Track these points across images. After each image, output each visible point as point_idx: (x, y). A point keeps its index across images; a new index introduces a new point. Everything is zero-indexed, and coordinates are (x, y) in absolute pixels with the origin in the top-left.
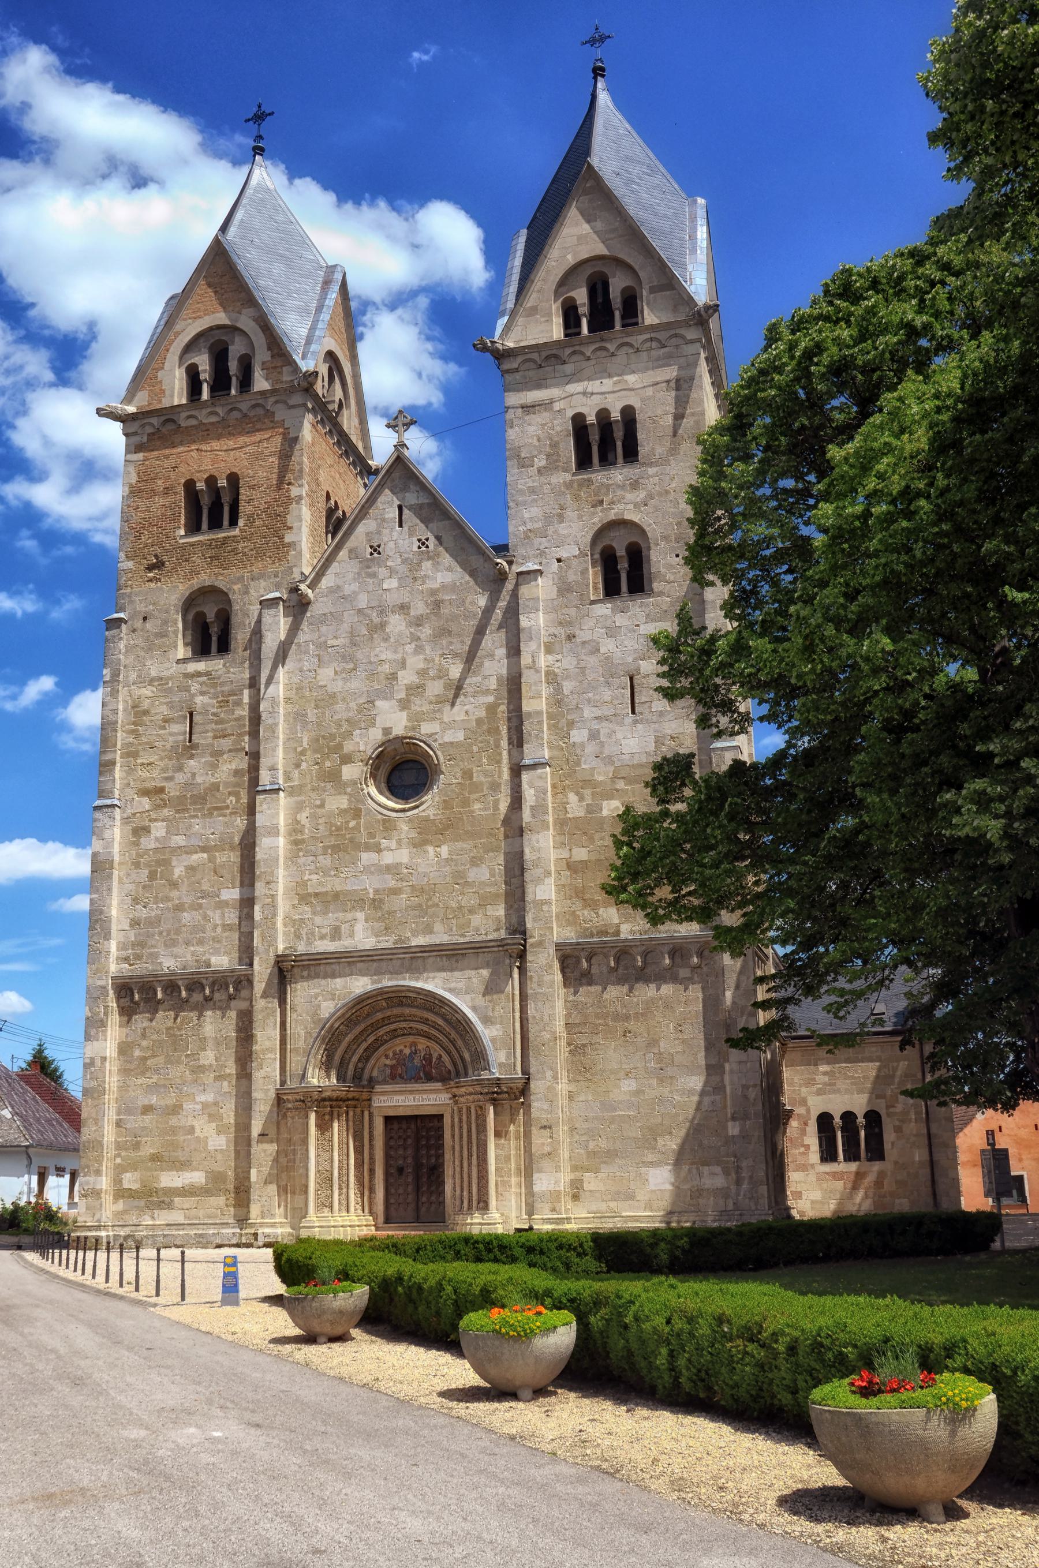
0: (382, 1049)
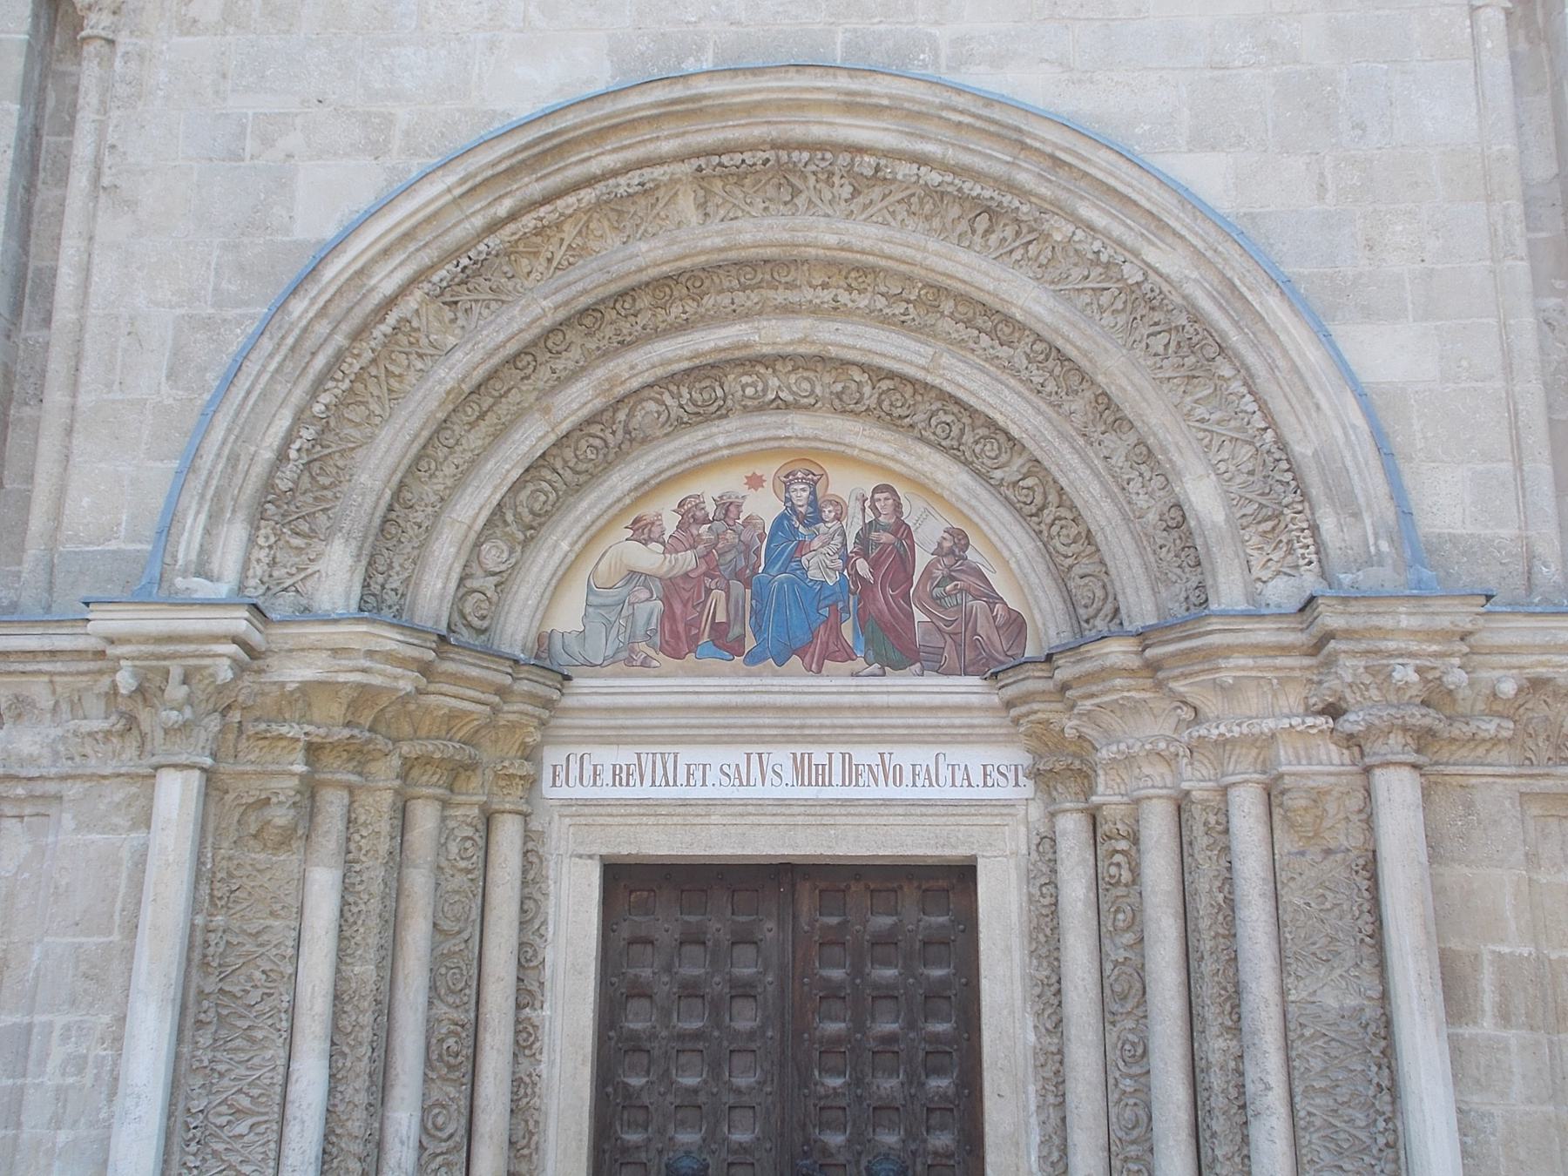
0: (621, 481)
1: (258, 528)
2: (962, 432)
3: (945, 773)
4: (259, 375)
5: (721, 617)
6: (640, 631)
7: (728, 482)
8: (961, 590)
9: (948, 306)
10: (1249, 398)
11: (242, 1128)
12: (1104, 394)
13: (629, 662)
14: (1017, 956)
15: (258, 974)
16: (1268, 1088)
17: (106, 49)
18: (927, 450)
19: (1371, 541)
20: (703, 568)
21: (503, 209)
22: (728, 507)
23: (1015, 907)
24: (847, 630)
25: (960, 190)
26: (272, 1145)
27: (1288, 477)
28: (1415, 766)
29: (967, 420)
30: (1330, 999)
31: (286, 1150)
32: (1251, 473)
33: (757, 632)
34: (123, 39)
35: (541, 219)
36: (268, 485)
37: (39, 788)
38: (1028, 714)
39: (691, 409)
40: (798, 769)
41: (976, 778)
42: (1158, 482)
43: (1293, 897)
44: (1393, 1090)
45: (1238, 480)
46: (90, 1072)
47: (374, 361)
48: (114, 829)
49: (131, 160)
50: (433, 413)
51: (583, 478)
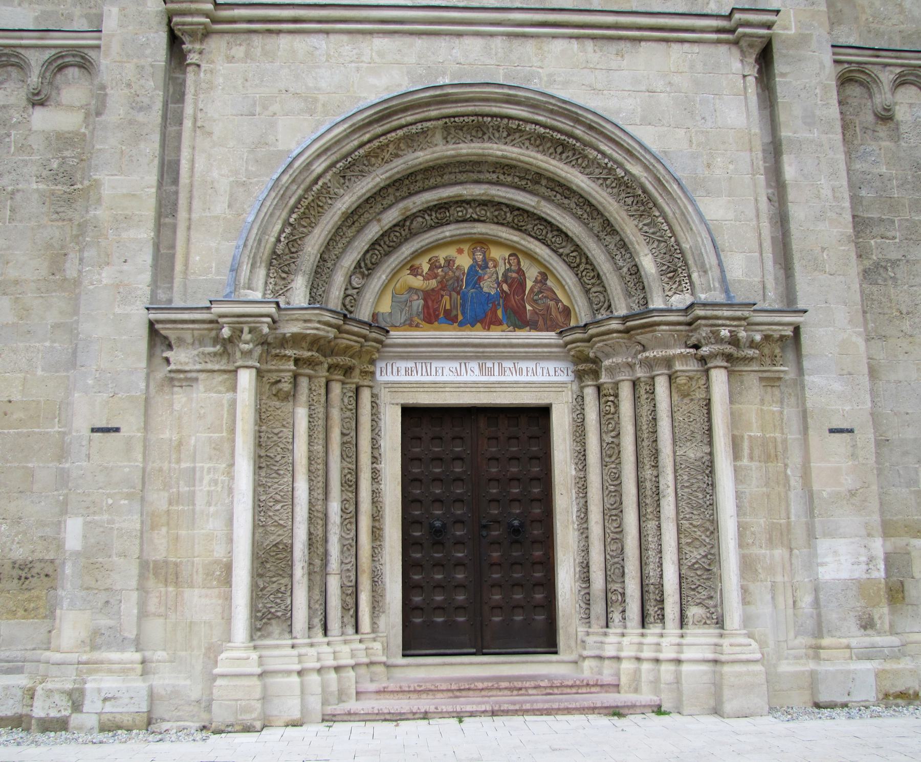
0: (406, 250)
1: (269, 270)
2: (547, 233)
3: (540, 371)
4: (270, 206)
5: (448, 307)
6: (414, 313)
7: (451, 252)
8: (545, 297)
9: (544, 182)
10: (665, 224)
11: (278, 507)
12: (608, 220)
13: (411, 325)
14: (568, 442)
15: (279, 449)
16: (668, 487)
17: (196, 69)
18: (532, 240)
19: (711, 282)
20: (440, 287)
21: (367, 137)
22: (449, 262)
23: (567, 423)
24: (500, 313)
25: (552, 136)
26: (290, 514)
27: (680, 256)
28: (726, 368)
29: (549, 229)
30: (691, 455)
31: (295, 515)
32: (665, 254)
33: (463, 313)
34: (204, 66)
35: (380, 142)
36: (274, 252)
37: (189, 375)
38: (575, 348)
39: (437, 221)
40: (481, 370)
41: (552, 372)
42: (628, 256)
43: (679, 416)
44: (713, 485)
45: (660, 256)
46: (220, 485)
47: (313, 201)
48: (220, 392)
49: (209, 115)
50: (337, 222)
51: (391, 249)
